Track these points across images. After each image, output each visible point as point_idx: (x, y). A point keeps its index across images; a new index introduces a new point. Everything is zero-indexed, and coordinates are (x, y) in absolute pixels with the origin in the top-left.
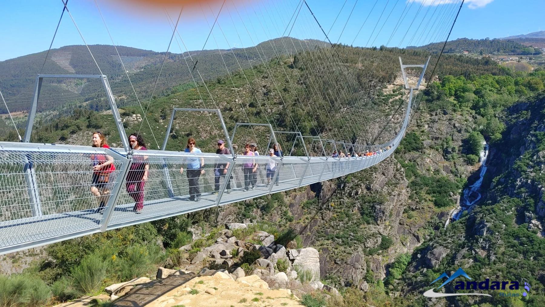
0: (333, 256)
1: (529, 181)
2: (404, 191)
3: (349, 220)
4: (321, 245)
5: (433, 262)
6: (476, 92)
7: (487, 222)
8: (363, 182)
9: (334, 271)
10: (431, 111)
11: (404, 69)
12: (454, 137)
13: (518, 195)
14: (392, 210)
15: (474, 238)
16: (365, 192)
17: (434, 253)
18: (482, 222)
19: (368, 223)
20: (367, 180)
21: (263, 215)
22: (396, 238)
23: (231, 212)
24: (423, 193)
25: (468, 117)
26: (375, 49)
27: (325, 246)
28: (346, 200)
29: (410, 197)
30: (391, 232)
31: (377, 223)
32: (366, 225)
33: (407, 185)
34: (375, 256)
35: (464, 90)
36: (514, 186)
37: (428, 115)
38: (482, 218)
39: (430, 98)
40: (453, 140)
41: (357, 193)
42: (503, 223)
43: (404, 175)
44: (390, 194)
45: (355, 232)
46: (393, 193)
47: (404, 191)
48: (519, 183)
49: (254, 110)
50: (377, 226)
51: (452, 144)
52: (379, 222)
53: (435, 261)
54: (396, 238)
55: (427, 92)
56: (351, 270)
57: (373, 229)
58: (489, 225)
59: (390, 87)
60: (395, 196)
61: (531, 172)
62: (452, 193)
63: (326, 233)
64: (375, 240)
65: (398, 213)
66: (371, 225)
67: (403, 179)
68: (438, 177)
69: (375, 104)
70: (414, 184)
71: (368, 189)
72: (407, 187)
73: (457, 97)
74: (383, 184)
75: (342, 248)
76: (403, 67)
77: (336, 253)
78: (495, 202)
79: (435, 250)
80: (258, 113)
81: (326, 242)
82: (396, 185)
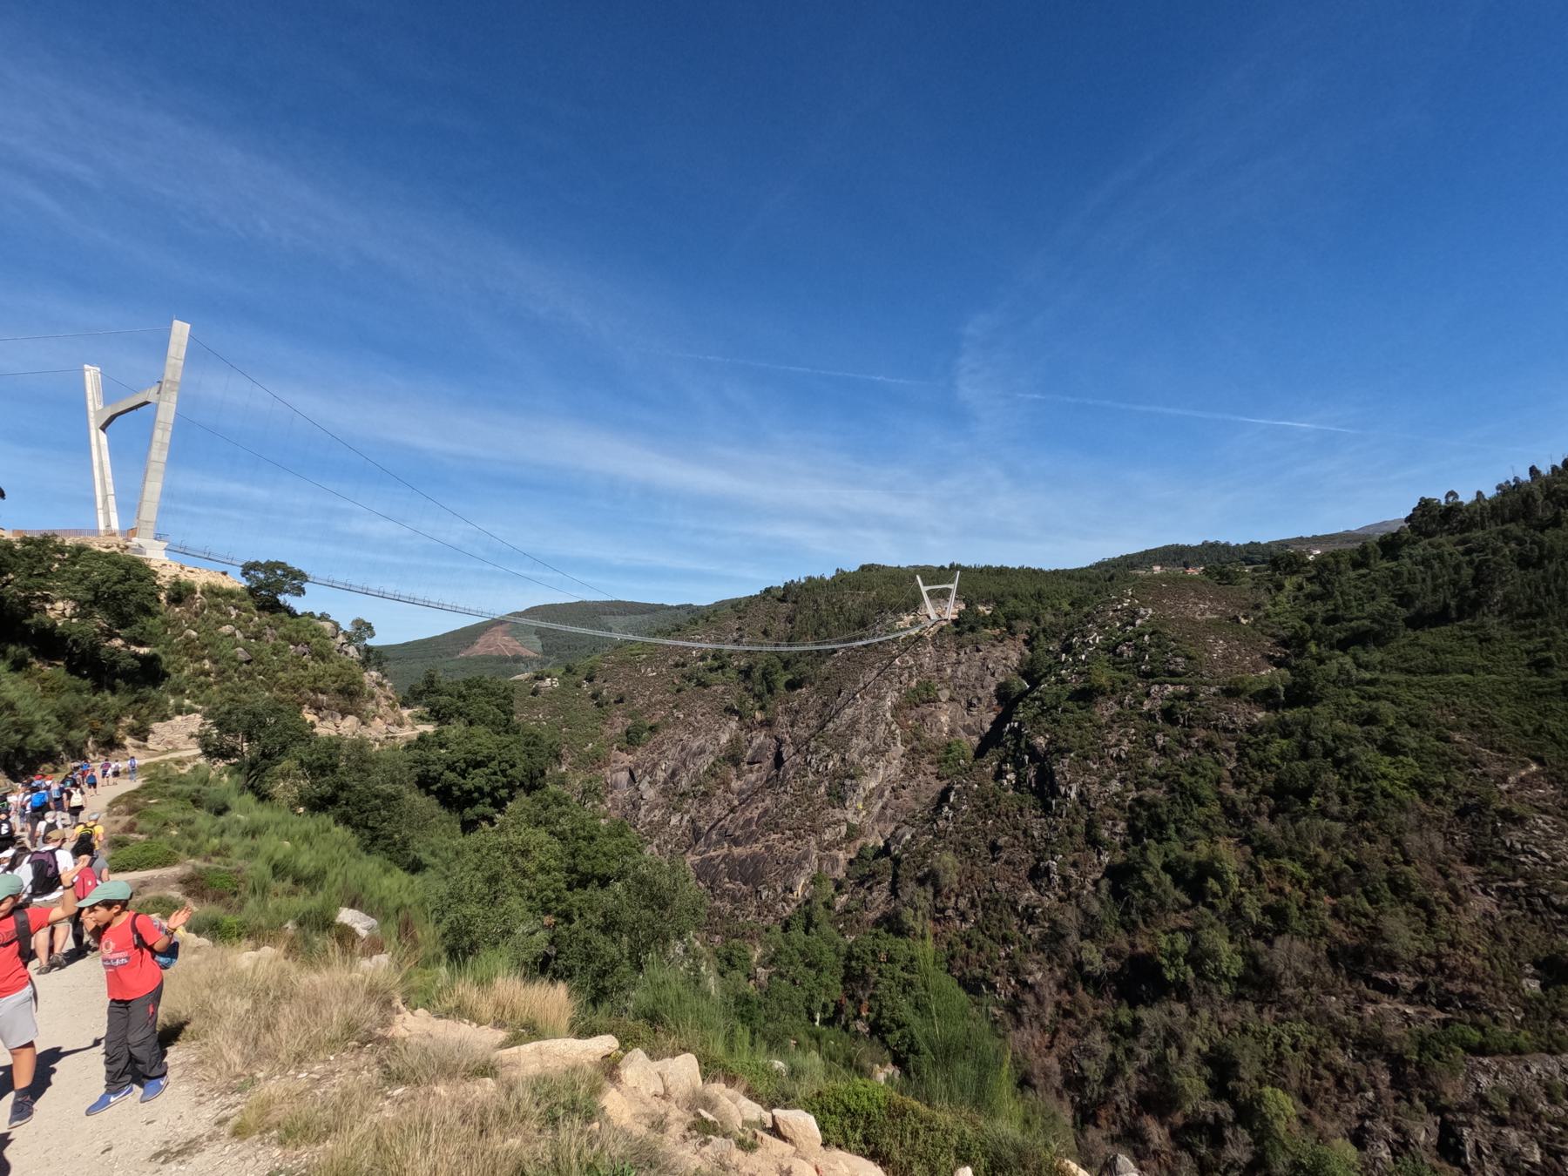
3: (810, 805)
5: (892, 848)
6: (1037, 621)
11: (928, 592)
12: (985, 684)
24: (924, 763)
26: (942, 568)
34: (834, 852)
44: (872, 766)
45: (813, 820)
49: (716, 664)
52: (847, 804)
59: (908, 619)
62: (962, 761)
63: (777, 825)
65: (883, 791)
67: (895, 744)
70: (913, 750)
75: (789, 843)
76: (924, 589)
80: (722, 667)
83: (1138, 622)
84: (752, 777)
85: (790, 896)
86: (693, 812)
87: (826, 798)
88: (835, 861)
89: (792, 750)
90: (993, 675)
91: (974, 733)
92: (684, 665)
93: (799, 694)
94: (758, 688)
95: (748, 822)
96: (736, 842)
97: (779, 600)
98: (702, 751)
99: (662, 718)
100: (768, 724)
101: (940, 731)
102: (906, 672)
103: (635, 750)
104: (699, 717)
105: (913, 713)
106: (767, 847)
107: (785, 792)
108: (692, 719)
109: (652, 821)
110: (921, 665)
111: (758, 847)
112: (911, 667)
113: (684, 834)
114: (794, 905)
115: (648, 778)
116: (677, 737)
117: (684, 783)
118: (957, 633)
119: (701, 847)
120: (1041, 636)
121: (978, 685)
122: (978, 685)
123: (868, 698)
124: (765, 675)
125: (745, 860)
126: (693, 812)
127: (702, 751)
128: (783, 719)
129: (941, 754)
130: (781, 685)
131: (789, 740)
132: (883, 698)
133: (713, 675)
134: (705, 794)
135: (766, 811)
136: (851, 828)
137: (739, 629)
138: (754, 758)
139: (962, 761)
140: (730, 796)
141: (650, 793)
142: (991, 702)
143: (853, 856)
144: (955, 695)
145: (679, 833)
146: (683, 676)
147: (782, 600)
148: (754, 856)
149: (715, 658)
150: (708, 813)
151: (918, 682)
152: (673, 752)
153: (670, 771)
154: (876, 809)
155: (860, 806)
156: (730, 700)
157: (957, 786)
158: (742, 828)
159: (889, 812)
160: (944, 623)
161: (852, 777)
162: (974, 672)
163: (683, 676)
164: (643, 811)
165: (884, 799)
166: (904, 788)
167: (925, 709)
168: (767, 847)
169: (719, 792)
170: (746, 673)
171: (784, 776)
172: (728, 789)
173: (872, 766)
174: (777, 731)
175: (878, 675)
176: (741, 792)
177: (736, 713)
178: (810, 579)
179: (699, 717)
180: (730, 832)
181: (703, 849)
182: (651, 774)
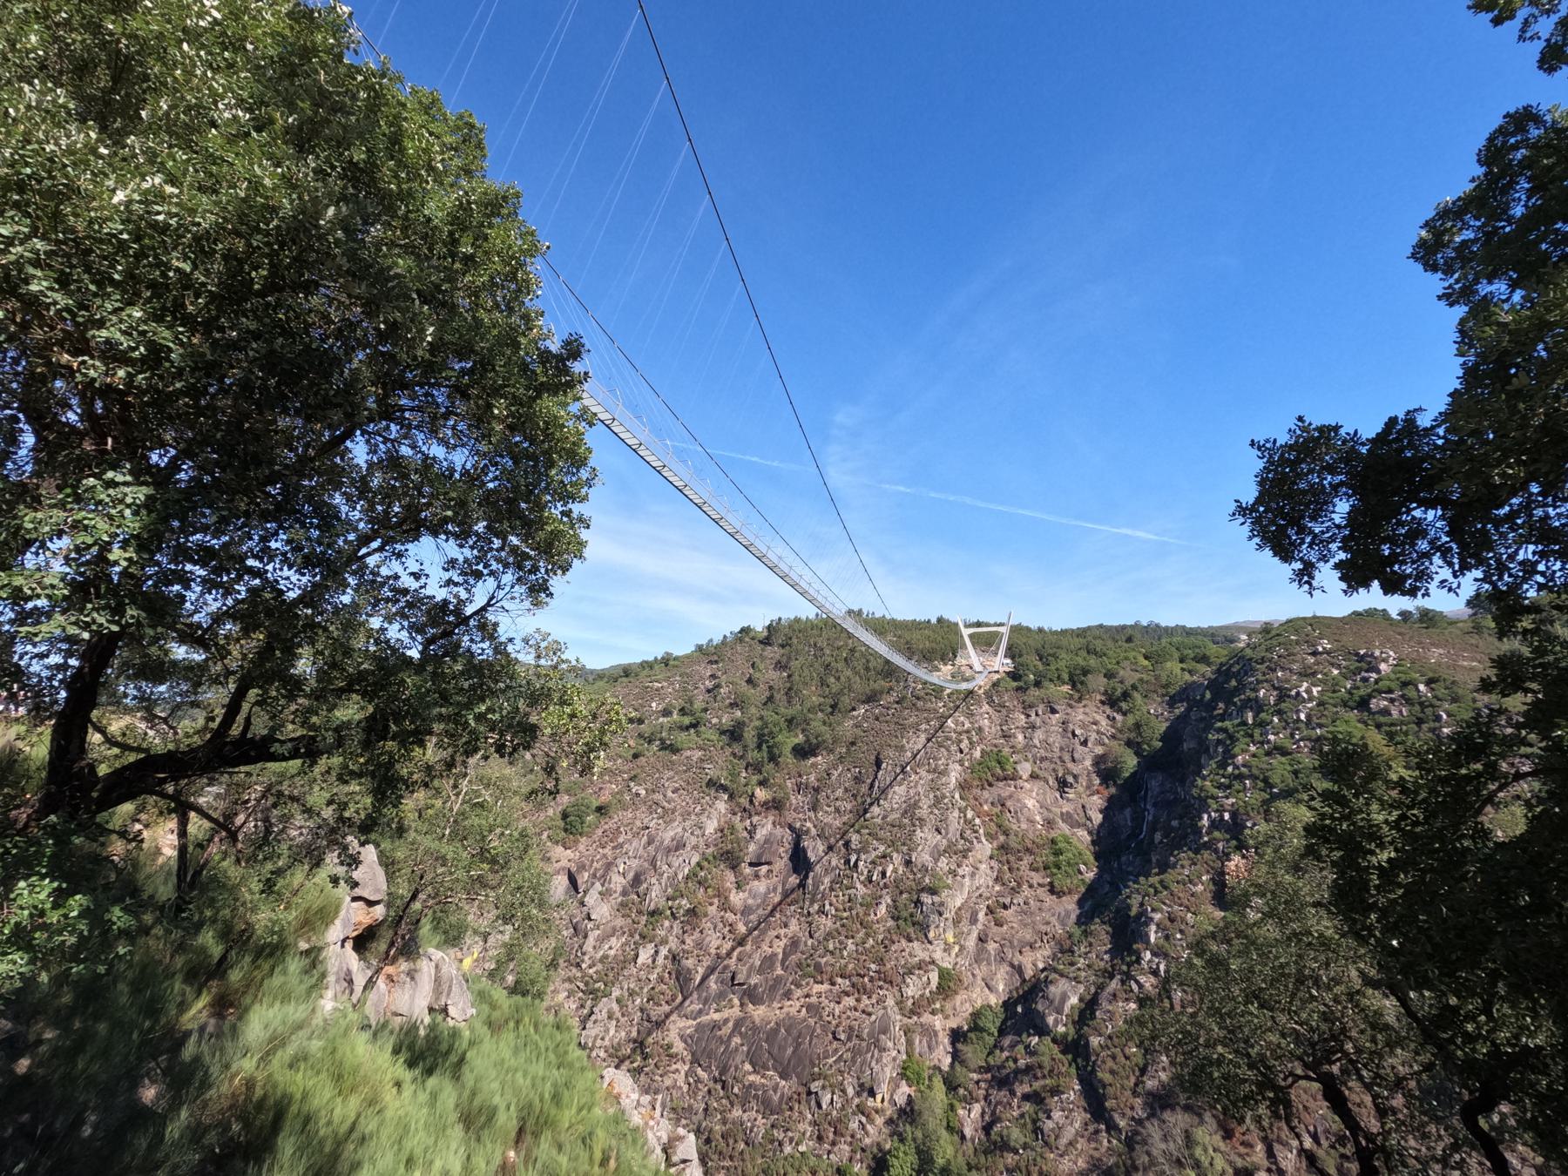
0: (829, 1023)
1: (1227, 816)
2: (983, 867)
3: (868, 935)
4: (808, 996)
5: (1050, 1020)
7: (1153, 910)
8: (898, 852)
9: (831, 1061)
10: (1027, 708)
11: (971, 636)
12: (1076, 756)
13: (1207, 846)
14: (960, 909)
15: (1131, 952)
16: (901, 872)
17: (1051, 996)
18: (1143, 913)
19: (910, 940)
20: (904, 844)
21: (684, 932)
22: (973, 975)
23: (614, 930)
25: (1098, 717)
27: (814, 1000)
28: (861, 890)
29: (997, 880)
30: (959, 959)
31: (926, 937)
32: (904, 942)
33: (989, 853)
34: (926, 1018)
35: (1085, 672)
36: (1197, 832)
37: (1023, 717)
38: (1142, 904)
39: (1021, 684)
40: (1074, 760)
41: (884, 874)
42: (1189, 910)
43: (981, 831)
44: (954, 873)
45: (881, 961)
46: (960, 872)
47: (983, 867)
48: (1205, 821)
49: (687, 720)
50: (929, 946)
51: (1075, 769)
52: (931, 935)
53: (1055, 1015)
54: (973, 975)
55: (1014, 675)
56: (869, 1055)
57: (918, 951)
58: (1157, 916)
60: (963, 876)
61: (1227, 797)
62: (1082, 867)
63: (818, 967)
64: (925, 979)
66: (916, 944)
68: (1053, 834)
69: (918, 698)
71: (908, 863)
72: (991, 858)
73: (1074, 687)
74: (939, 851)
75: (849, 1001)
77: (837, 1013)
78: (1164, 867)
79: (1052, 989)
80: (694, 726)
81: (817, 988)
82: (965, 854)
83: (1383, 666)
84: (760, 886)
85: (870, 1102)
86: (673, 943)
87: (891, 923)
88: (930, 1033)
89: (821, 847)
90: (1085, 743)
91: (1079, 825)
92: (640, 721)
93: (814, 765)
94: (753, 755)
95: (769, 961)
96: (751, 996)
97: (761, 642)
98: (680, 845)
99: (613, 795)
100: (776, 805)
101: (1031, 821)
102: (964, 737)
103: (576, 842)
104: (670, 794)
105: (986, 794)
106: (809, 1007)
107: (821, 911)
108: (658, 797)
109: (605, 957)
110: (980, 729)
111: (793, 1007)
112: (968, 732)
113: (661, 980)
114: (879, 1121)
115: (598, 885)
116: (638, 823)
117: (656, 895)
118: (1018, 689)
119: (693, 1006)
120: (1136, 695)
121: (1067, 757)
122: (1067, 757)
123: (923, 773)
124: (761, 740)
125: (775, 1031)
126: (673, 943)
127: (680, 845)
128: (795, 800)
129: (1045, 856)
130: (787, 750)
131: (814, 831)
132: (944, 773)
133: (684, 735)
134: (692, 912)
135: (794, 943)
136: (944, 975)
137: (713, 676)
138: (760, 856)
139: (1082, 867)
140: (730, 916)
141: (602, 911)
142: (1090, 780)
143: (953, 1023)
144: (1038, 772)
145: (653, 977)
146: (640, 736)
147: (766, 642)
148: (789, 1024)
149: (683, 711)
150: (699, 945)
151: (983, 751)
152: (636, 845)
153: (631, 875)
154: (971, 942)
155: (951, 940)
156: (712, 771)
157: (1157, 916)
158: (760, 971)
159: (992, 947)
160: (996, 676)
161: (933, 891)
162: (1057, 740)
163: (640, 736)
164: (591, 941)
165: (980, 926)
166: (1005, 907)
167: (1003, 789)
168: (809, 1007)
169: (712, 910)
170: (734, 734)
171: (816, 886)
172: (725, 906)
173: (954, 873)
174: (790, 816)
175: (929, 740)
176: (747, 910)
177: (724, 788)
178: (797, 620)
179: (670, 794)
180: (740, 978)
181: (697, 1007)
182: (604, 879)
